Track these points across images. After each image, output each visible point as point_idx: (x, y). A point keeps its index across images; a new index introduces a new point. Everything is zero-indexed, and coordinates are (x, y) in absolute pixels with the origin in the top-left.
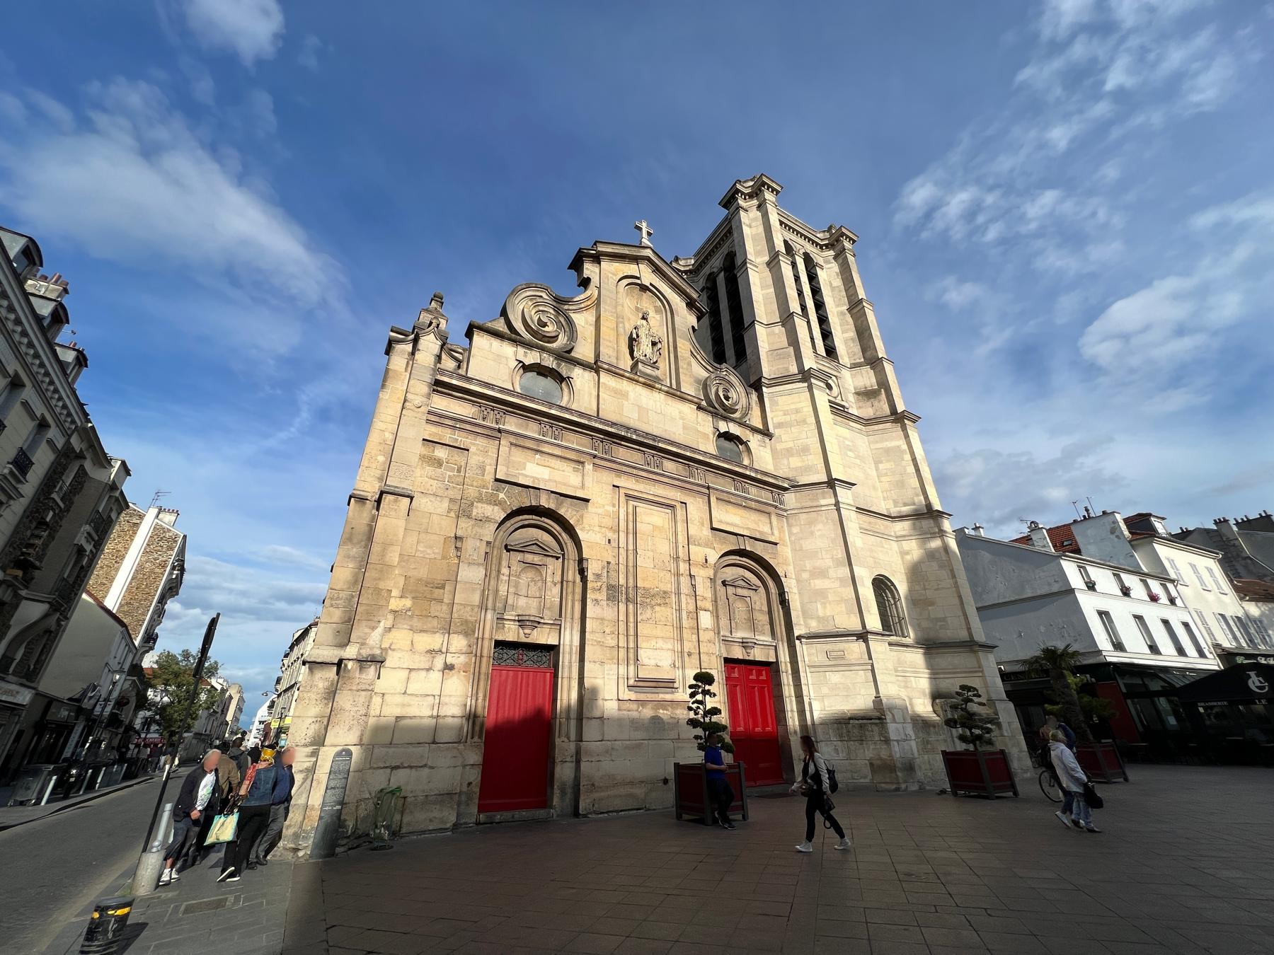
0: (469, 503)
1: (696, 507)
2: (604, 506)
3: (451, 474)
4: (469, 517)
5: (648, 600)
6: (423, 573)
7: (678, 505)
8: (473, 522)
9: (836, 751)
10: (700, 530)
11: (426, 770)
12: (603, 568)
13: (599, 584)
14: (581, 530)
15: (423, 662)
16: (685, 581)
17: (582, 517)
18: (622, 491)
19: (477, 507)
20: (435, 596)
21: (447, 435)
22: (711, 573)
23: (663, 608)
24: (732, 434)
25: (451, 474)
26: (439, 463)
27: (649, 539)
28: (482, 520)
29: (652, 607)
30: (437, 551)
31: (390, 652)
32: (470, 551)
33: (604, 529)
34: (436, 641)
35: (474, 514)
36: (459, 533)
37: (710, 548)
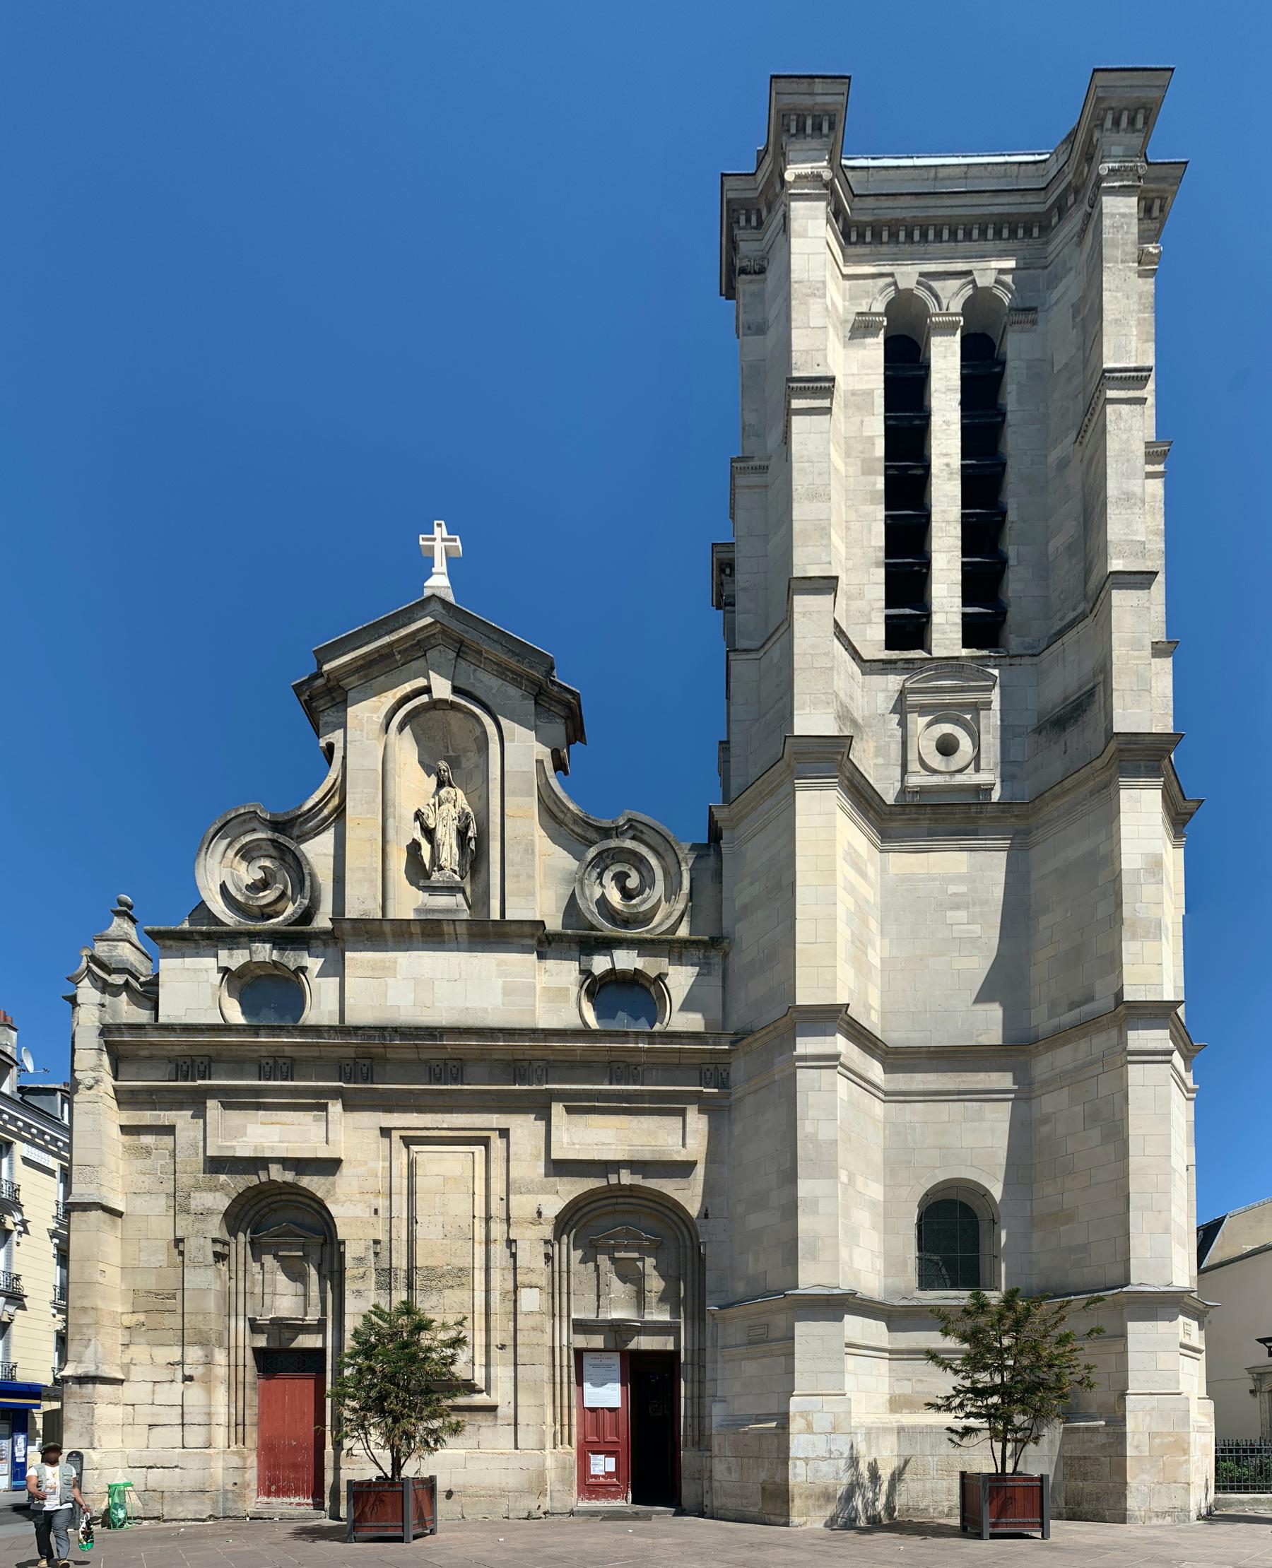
0: (185, 1195)
1: (525, 1128)
2: (366, 1163)
3: (163, 1162)
4: (188, 1212)
5: (434, 1283)
6: (150, 1282)
7: (494, 1136)
8: (192, 1218)
9: (729, 1469)
10: (529, 1166)
11: (177, 1470)
12: (367, 1249)
13: (361, 1270)
14: (333, 1203)
15: (165, 1375)
16: (499, 1250)
17: (333, 1184)
18: (395, 1134)
19: (195, 1198)
20: (168, 1307)
21: (147, 1117)
22: (547, 1231)
23: (457, 1291)
24: (624, 972)
25: (163, 1162)
26: (148, 1151)
27: (437, 1200)
28: (205, 1213)
29: (440, 1291)
30: (161, 1258)
31: (132, 1367)
32: (194, 1254)
33: (367, 1196)
34: (174, 1354)
35: (193, 1207)
36: (179, 1234)
37: (549, 1193)
